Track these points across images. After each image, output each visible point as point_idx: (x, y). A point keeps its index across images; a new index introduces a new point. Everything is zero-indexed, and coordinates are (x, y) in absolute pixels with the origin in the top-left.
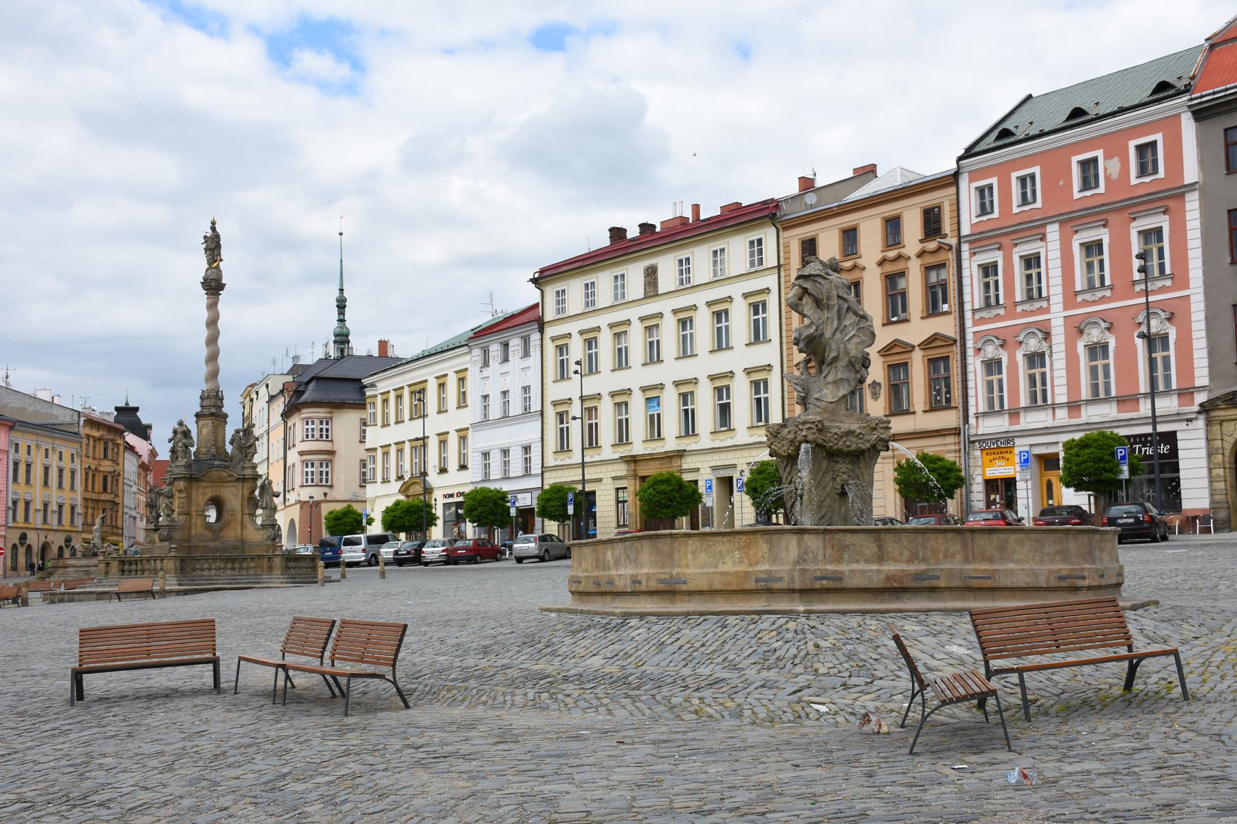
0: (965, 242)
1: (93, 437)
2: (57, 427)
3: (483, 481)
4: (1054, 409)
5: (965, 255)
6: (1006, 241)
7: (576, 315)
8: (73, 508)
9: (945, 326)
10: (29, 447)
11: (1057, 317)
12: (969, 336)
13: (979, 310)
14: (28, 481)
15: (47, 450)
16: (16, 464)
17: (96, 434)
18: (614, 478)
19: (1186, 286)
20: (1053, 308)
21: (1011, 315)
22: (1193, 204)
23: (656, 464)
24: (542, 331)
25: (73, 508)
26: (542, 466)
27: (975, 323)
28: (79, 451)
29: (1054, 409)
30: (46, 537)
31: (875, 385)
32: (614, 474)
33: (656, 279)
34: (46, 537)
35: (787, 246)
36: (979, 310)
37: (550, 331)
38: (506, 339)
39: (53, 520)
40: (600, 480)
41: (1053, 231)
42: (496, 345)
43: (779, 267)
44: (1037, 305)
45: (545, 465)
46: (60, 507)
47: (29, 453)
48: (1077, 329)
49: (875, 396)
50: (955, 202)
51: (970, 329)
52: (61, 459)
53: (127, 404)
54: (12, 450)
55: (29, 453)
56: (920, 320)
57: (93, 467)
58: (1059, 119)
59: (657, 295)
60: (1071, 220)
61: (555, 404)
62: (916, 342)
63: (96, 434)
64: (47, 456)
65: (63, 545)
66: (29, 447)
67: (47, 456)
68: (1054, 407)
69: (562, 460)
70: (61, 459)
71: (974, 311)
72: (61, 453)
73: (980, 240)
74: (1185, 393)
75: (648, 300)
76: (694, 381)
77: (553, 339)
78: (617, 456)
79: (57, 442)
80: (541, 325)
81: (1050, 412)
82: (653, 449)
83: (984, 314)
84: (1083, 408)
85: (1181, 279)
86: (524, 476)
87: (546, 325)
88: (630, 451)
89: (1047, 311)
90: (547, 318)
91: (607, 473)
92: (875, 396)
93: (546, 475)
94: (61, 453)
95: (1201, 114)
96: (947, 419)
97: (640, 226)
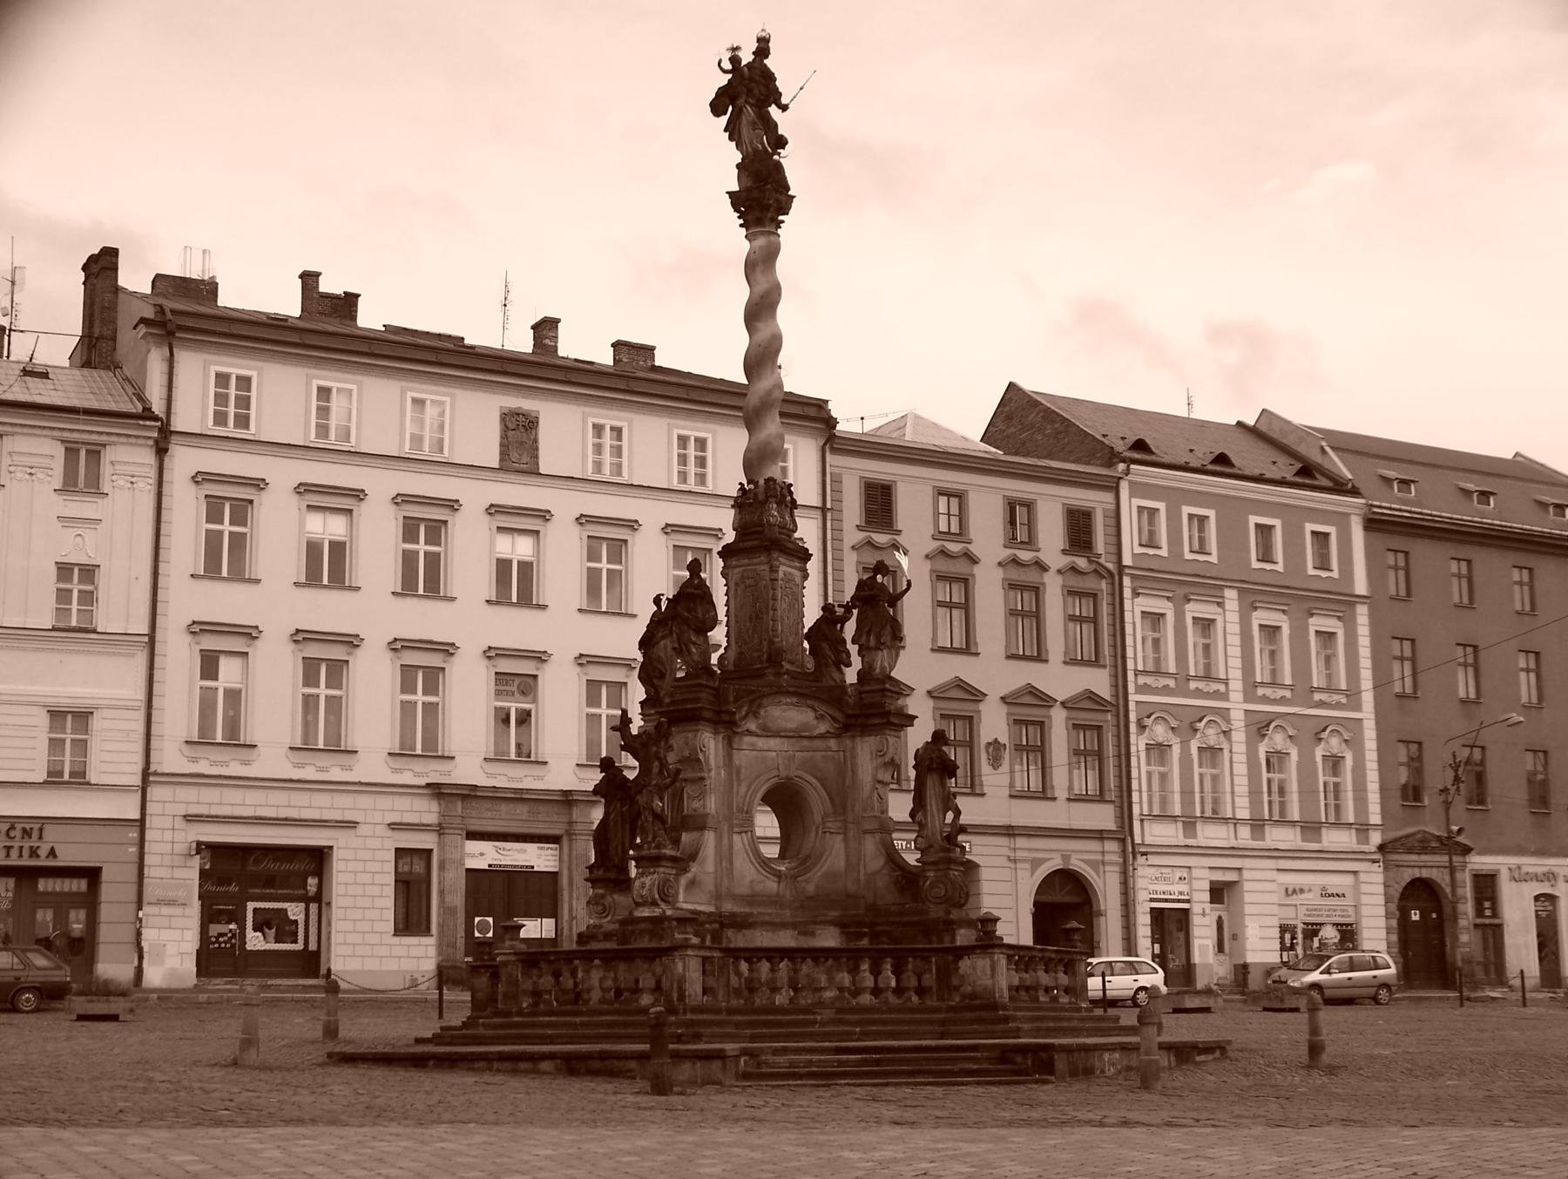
0: (1128, 574)
3: (54, 780)
4: (1235, 824)
5: (1127, 593)
6: (1181, 591)
7: (289, 445)
9: (1099, 681)
11: (1237, 706)
12: (1132, 706)
13: (1145, 672)
18: (394, 826)
19: (1358, 708)
20: (1233, 696)
21: (1182, 691)
22: (1362, 614)
23: (522, 810)
24: (161, 451)
26: (146, 773)
27: (1141, 689)
29: (1235, 824)
31: (995, 745)
32: (396, 818)
33: (536, 441)
35: (837, 480)
36: (1145, 672)
37: (183, 460)
38: (104, 438)
40: (352, 825)
41: (1231, 595)
42: (48, 441)
43: (823, 509)
44: (1214, 686)
45: (153, 768)
48: (1260, 727)
49: (995, 762)
50: (1113, 515)
51: (1133, 698)
56: (930, 652)
58: (1202, 457)
59: (535, 472)
60: (1255, 593)
61: (199, 628)
62: (1060, 695)
68: (1235, 822)
69: (214, 763)
71: (1137, 673)
73: (1152, 578)
74: (1363, 829)
75: (501, 476)
76: (584, 661)
77: (200, 478)
78: (423, 782)
80: (164, 439)
81: (1231, 827)
82: (510, 779)
83: (1149, 680)
84: (1267, 828)
85: (1353, 695)
86: (45, 782)
87: (174, 438)
88: (449, 773)
89: (1224, 696)
90: (178, 424)
91: (376, 812)
92: (995, 762)
93: (155, 792)
95: (1374, 524)
96: (1102, 817)
97: (613, 345)
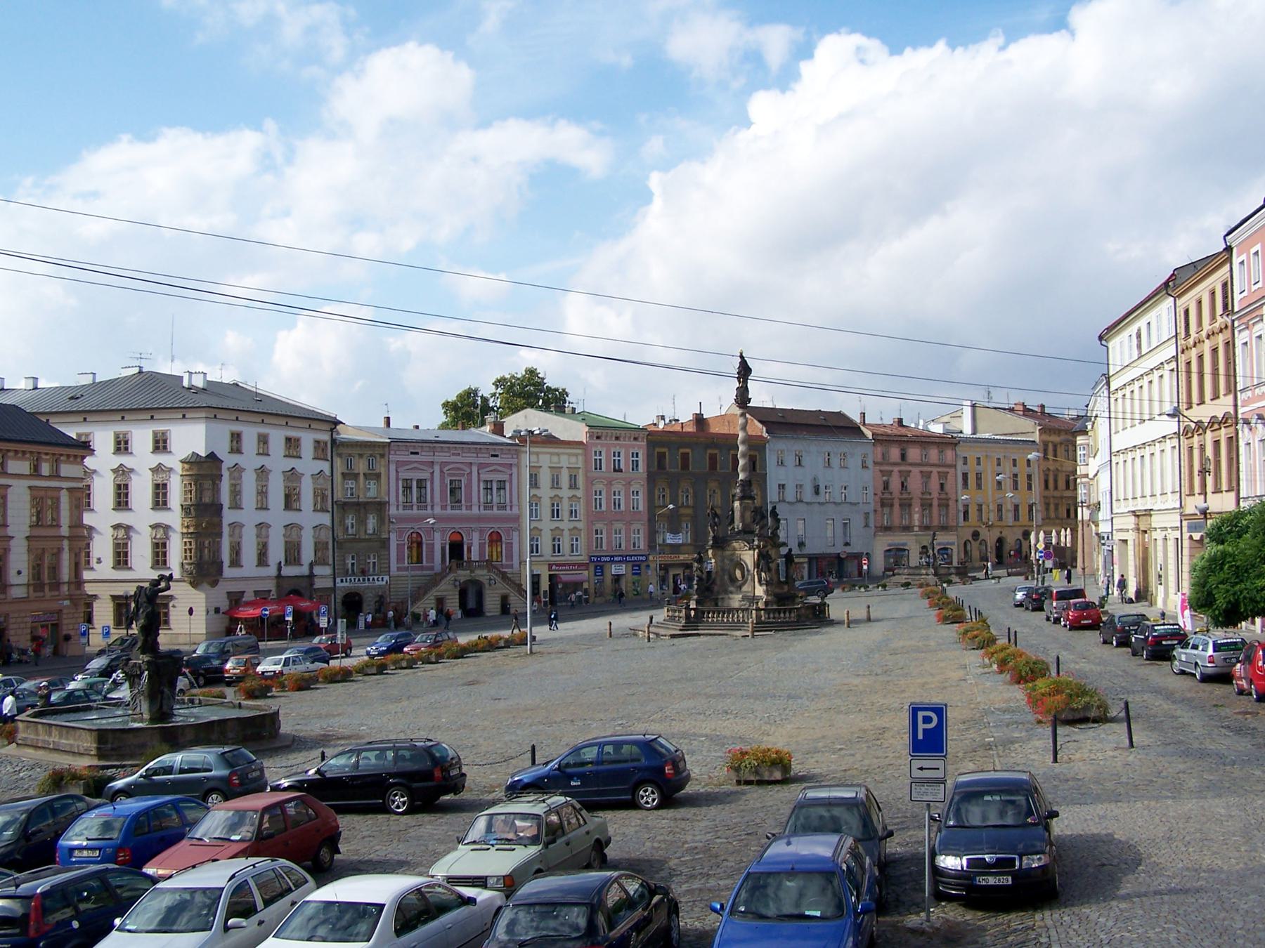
8: (1031, 507)
10: (979, 459)
14: (979, 486)
16: (965, 476)
25: (1031, 507)
30: (1001, 533)
34: (1001, 533)
39: (1009, 517)
46: (1016, 507)
47: (979, 464)
52: (1015, 465)
54: (960, 463)
55: (979, 464)
57: (1051, 468)
64: (999, 465)
65: (1021, 538)
66: (979, 459)
67: (999, 465)
70: (1015, 465)
94: (1014, 460)
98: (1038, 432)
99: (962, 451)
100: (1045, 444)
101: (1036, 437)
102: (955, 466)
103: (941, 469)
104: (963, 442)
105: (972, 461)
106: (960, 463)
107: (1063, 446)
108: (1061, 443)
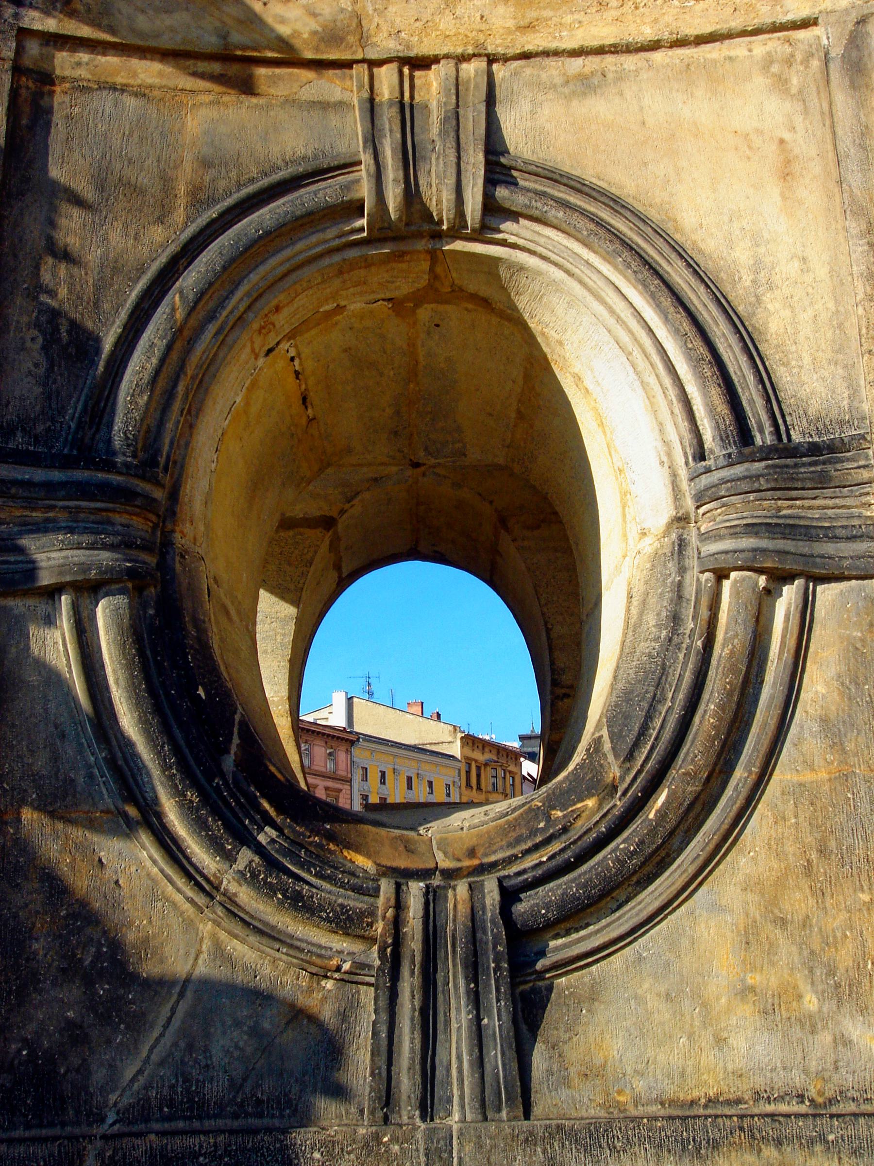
1: (476, 761)
2: (428, 747)
10: (383, 774)
15: (410, 779)
17: (480, 756)
28: (457, 780)
47: (383, 782)
53: (532, 731)
54: (357, 776)
55: (383, 782)
63: (480, 756)
64: (410, 787)
66: (383, 774)
67: (410, 787)
72: (430, 784)
79: (426, 767)
94: (430, 784)
98: (458, 743)
99: (360, 754)
100: (468, 761)
101: (456, 750)
102: (350, 781)
103: (330, 784)
104: (364, 740)
105: (374, 777)
106: (357, 776)
107: (489, 768)
108: (486, 765)
